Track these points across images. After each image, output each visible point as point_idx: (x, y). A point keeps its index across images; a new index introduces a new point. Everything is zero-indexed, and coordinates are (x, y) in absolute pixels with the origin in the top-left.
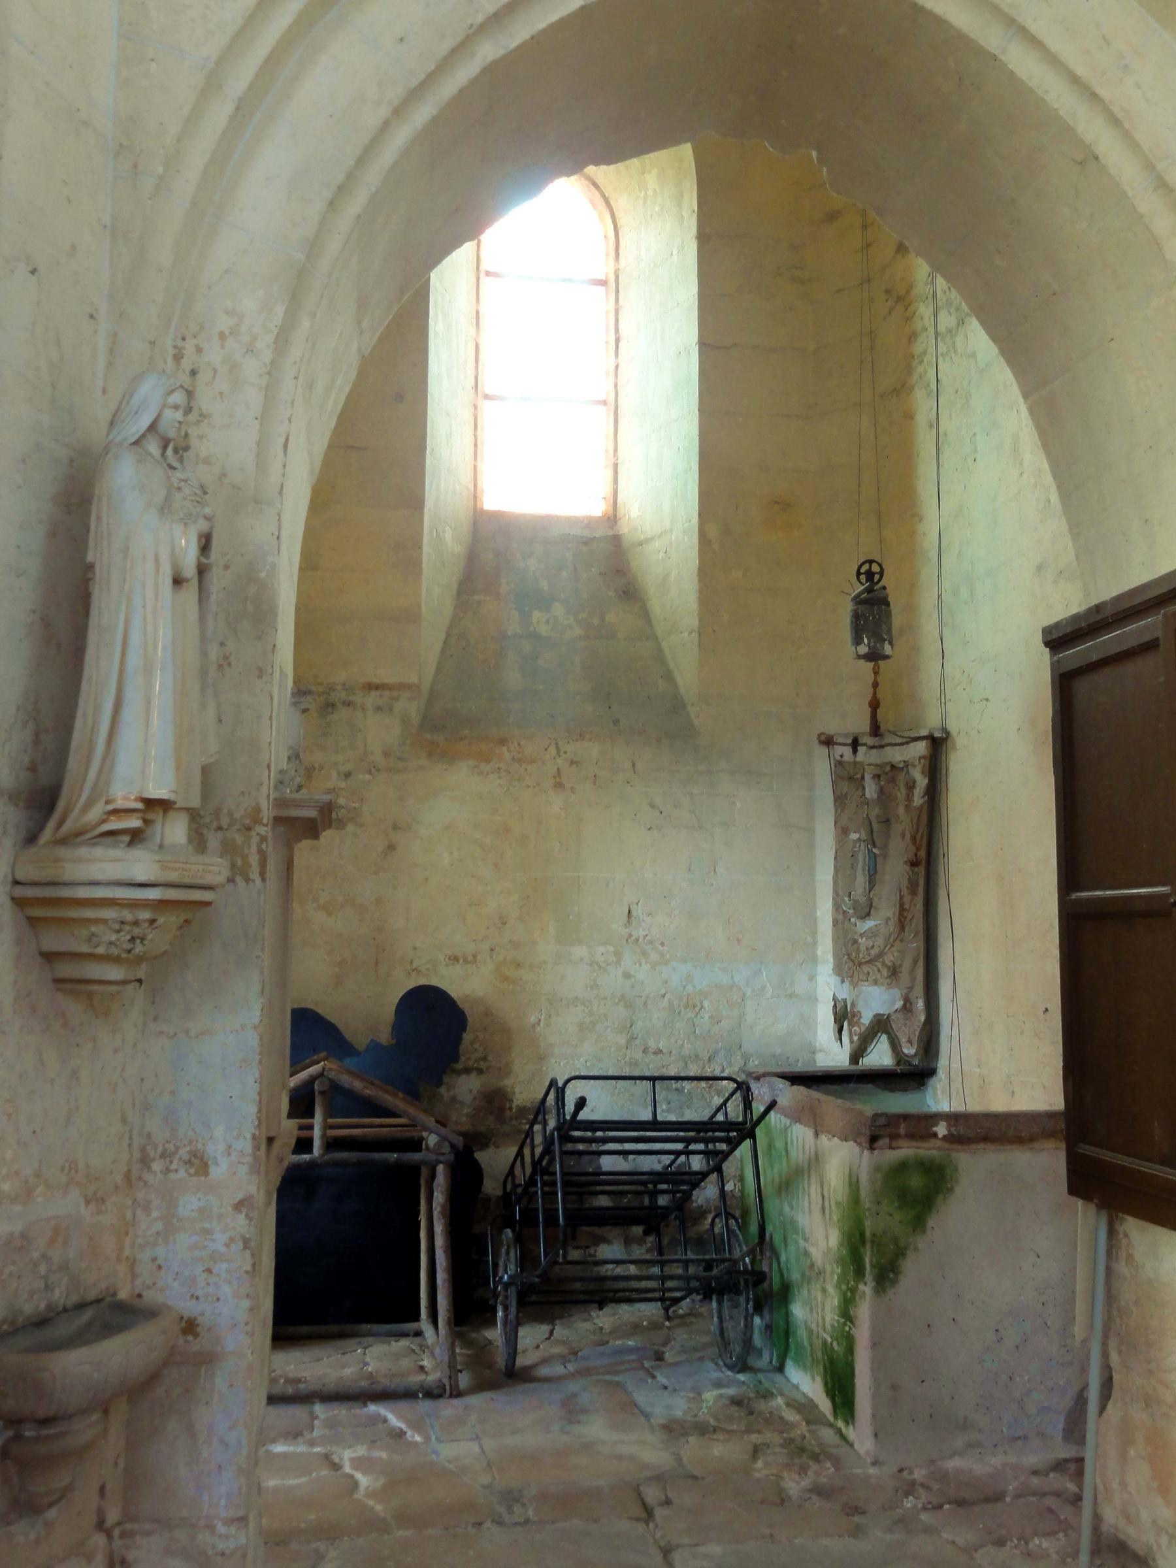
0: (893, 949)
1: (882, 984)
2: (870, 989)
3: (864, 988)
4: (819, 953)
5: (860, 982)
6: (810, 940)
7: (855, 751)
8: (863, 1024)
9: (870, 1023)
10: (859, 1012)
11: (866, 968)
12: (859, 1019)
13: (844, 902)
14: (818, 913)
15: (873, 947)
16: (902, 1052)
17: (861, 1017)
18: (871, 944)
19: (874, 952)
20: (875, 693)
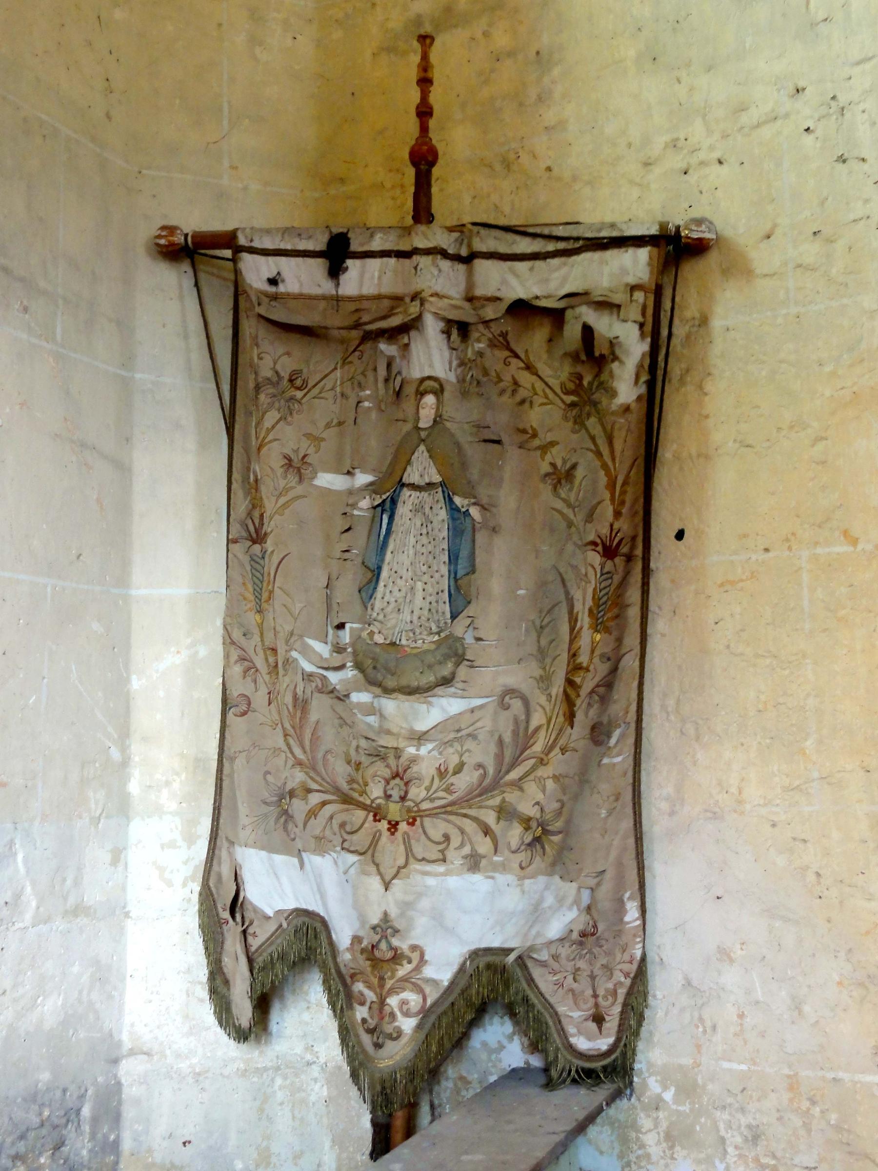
0: (541, 772)
1: (503, 868)
2: (454, 882)
3: (431, 881)
4: (134, 787)
5: (415, 866)
6: (115, 754)
7: (335, 271)
8: (435, 982)
9: (453, 983)
10: (414, 948)
11: (436, 828)
12: (418, 969)
13: (306, 651)
14: (136, 684)
15: (459, 769)
16: (571, 1048)
17: (422, 961)
18: (454, 760)
19: (464, 782)
20: (424, 129)
